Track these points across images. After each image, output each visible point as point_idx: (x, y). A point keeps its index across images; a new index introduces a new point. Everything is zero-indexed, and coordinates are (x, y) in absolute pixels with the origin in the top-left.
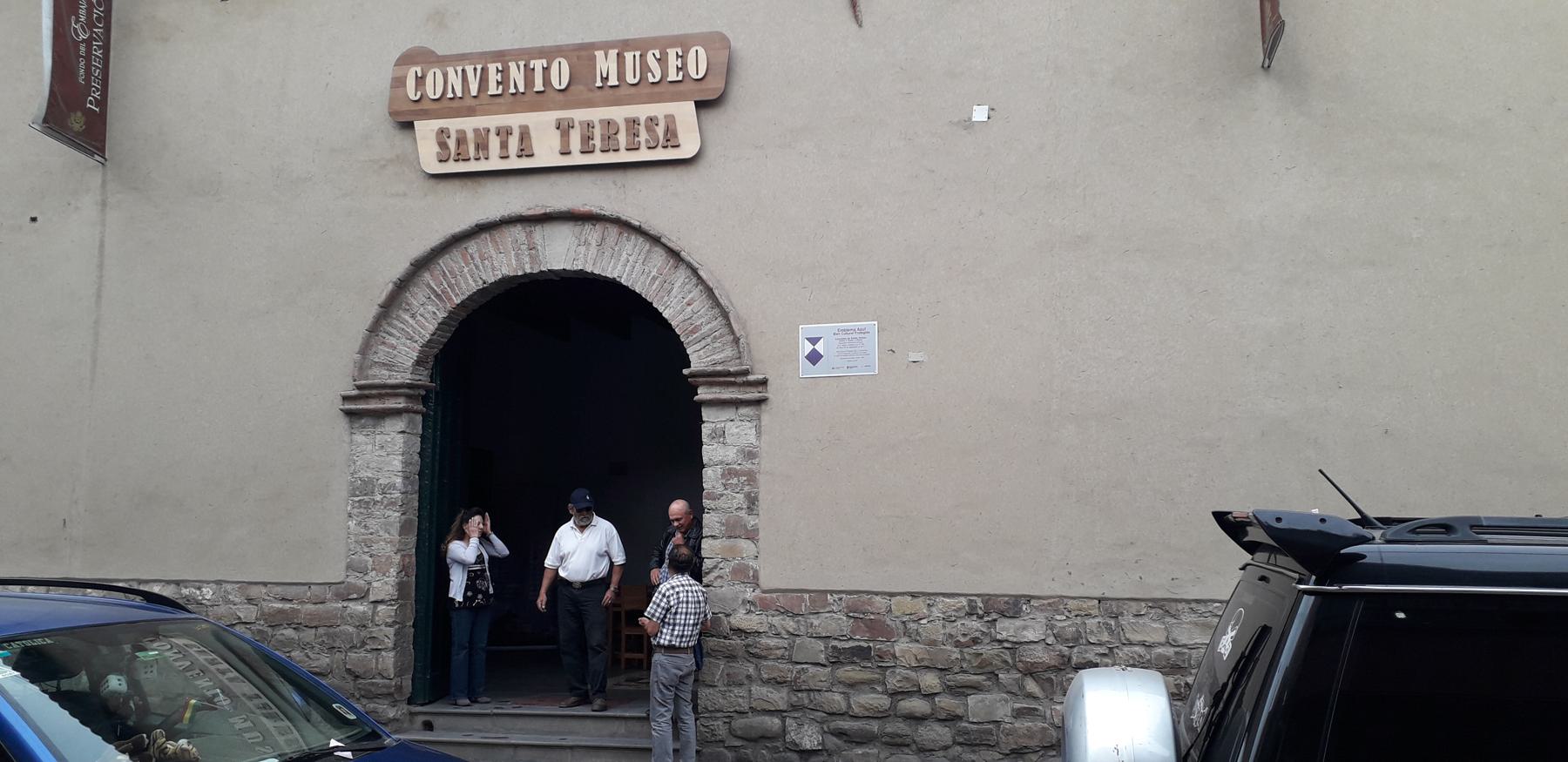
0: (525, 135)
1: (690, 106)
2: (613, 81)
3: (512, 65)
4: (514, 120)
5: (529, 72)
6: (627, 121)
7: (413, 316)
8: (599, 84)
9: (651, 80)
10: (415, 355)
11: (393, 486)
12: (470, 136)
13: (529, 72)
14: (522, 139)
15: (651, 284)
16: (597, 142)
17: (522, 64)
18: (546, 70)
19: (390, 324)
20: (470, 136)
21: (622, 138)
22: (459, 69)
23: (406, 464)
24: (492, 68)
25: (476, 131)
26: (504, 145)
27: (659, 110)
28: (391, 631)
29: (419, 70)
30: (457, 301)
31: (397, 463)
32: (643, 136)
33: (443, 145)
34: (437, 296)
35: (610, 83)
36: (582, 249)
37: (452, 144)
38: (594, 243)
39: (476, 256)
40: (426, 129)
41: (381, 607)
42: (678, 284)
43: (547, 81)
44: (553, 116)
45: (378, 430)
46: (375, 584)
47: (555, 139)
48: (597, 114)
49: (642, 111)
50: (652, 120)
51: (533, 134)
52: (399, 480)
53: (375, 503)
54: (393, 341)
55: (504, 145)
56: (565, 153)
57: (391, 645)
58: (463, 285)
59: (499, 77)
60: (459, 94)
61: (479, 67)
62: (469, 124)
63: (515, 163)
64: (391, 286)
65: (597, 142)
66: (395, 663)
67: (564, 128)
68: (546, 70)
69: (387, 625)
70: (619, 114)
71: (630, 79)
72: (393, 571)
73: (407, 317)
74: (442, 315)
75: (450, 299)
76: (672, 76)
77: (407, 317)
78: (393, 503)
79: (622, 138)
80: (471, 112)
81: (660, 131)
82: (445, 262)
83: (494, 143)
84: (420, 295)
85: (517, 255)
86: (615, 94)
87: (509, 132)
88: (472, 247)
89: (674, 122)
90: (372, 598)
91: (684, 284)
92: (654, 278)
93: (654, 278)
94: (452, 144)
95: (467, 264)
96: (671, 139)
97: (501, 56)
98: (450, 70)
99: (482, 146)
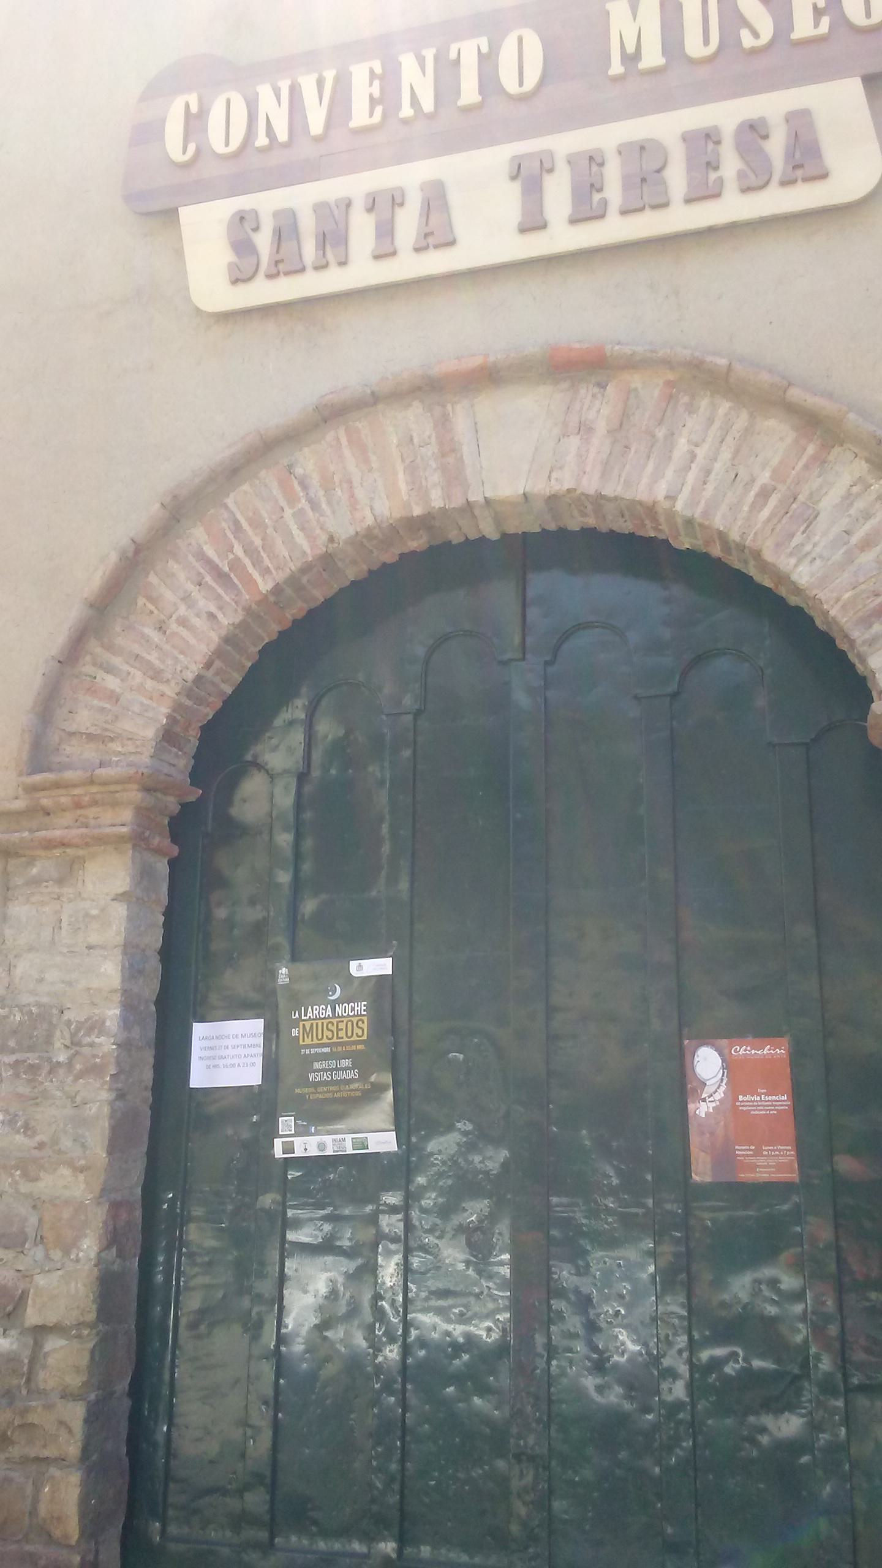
0: (435, 200)
1: (859, 80)
2: (652, 57)
3: (408, 62)
4: (411, 176)
5: (447, 70)
6: (686, 138)
7: (161, 628)
8: (616, 68)
9: (747, 40)
10: (162, 712)
11: (95, 1026)
12: (308, 225)
13: (447, 70)
14: (427, 209)
15: (756, 507)
16: (613, 192)
17: (429, 54)
18: (488, 61)
19: (110, 648)
20: (308, 225)
21: (677, 178)
22: (284, 85)
23: (132, 972)
24: (360, 74)
25: (321, 209)
26: (385, 231)
27: (772, 106)
28: (76, 1413)
29: (193, 100)
30: (265, 586)
31: (109, 972)
32: (731, 165)
33: (243, 247)
34: (221, 576)
35: (645, 63)
36: (574, 442)
37: (263, 241)
38: (601, 427)
39: (315, 480)
40: (205, 225)
41: (53, 1343)
42: (828, 502)
43: (489, 81)
44: (497, 157)
45: (68, 891)
46: (41, 1280)
47: (509, 201)
48: (608, 137)
49: (727, 115)
50: (754, 131)
51: (454, 199)
52: (112, 1013)
53: (55, 1067)
54: (112, 683)
55: (385, 231)
56: (533, 223)
57: (73, 1450)
58: (283, 551)
59: (376, 90)
60: (282, 136)
61: (330, 75)
62: (301, 198)
63: (408, 265)
64: (114, 557)
65: (613, 192)
66: (84, 1501)
67: (530, 177)
68: (488, 61)
69: (66, 1395)
70: (667, 127)
71: (694, 47)
72: (89, 1246)
73: (149, 631)
74: (228, 619)
75: (250, 582)
76: (804, 27)
77: (149, 631)
78: (93, 1070)
79: (677, 178)
80: (307, 172)
81: (776, 147)
82: (240, 500)
83: (362, 231)
84: (182, 576)
85: (412, 469)
86: (654, 89)
87: (396, 200)
88: (307, 461)
89: (811, 125)
90: (32, 1316)
91: (848, 499)
92: (765, 494)
93: (765, 494)
94: (263, 241)
95: (292, 500)
96: (806, 160)
97: (384, 47)
98: (265, 92)
99: (333, 239)
